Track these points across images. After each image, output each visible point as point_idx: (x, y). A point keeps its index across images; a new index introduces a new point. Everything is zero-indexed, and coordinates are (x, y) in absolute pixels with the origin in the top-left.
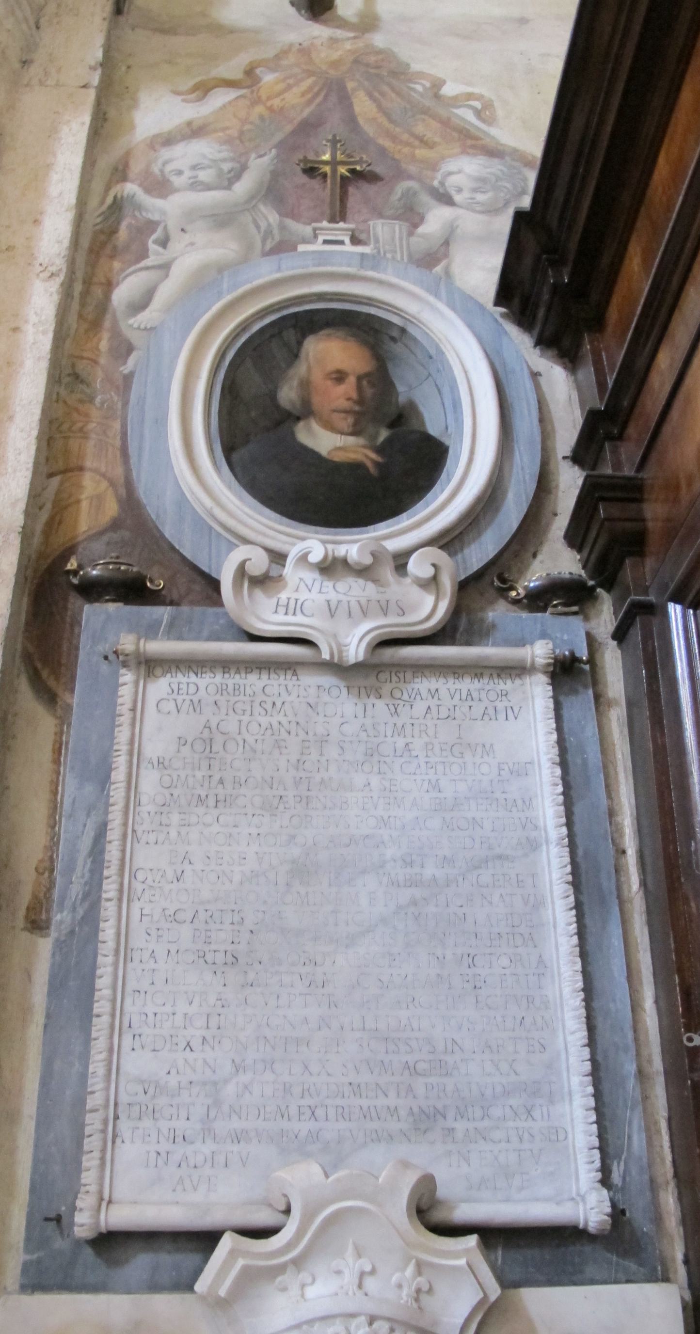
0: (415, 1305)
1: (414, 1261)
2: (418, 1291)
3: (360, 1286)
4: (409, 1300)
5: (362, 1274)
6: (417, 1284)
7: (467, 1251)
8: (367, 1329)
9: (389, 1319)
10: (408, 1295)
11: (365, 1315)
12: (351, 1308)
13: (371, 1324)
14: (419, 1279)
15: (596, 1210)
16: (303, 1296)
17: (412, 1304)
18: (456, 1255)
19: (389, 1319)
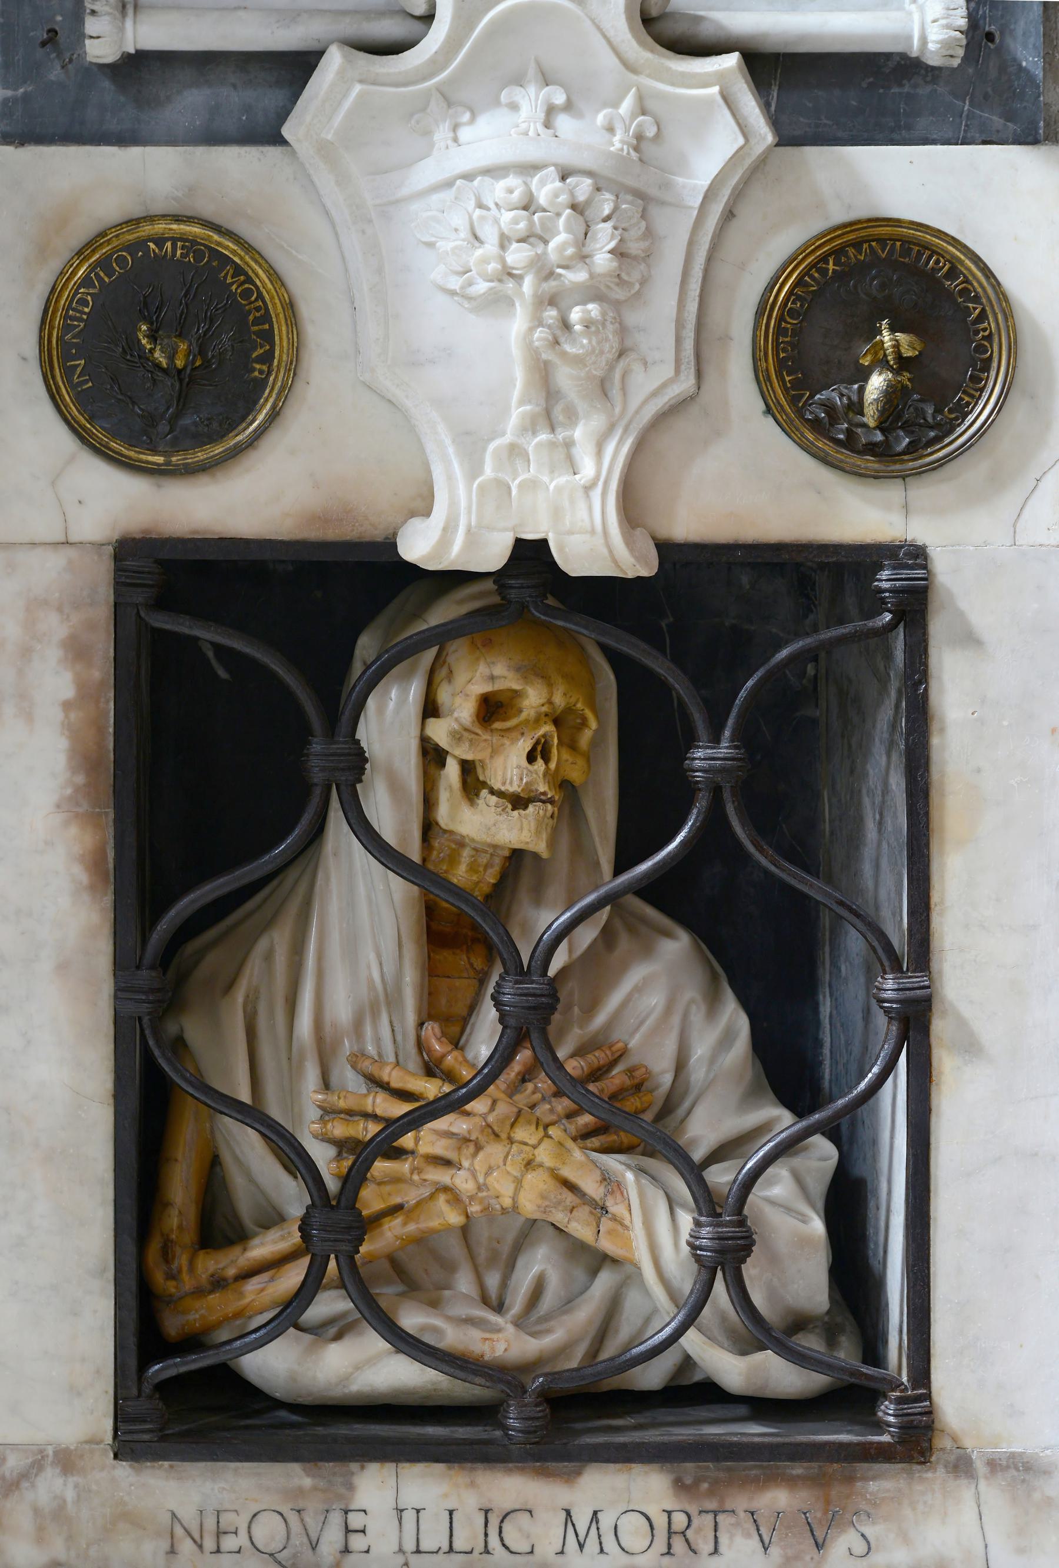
0: (634, 155)
1: (634, 90)
2: (639, 137)
3: (548, 124)
4: (625, 147)
5: (551, 111)
6: (639, 125)
7: (720, 78)
8: (558, 184)
9: (589, 174)
10: (623, 142)
11: (555, 165)
12: (532, 153)
13: (563, 178)
14: (641, 118)
15: (944, 22)
16: (455, 140)
17: (628, 153)
18: (704, 82)
19: (589, 174)
